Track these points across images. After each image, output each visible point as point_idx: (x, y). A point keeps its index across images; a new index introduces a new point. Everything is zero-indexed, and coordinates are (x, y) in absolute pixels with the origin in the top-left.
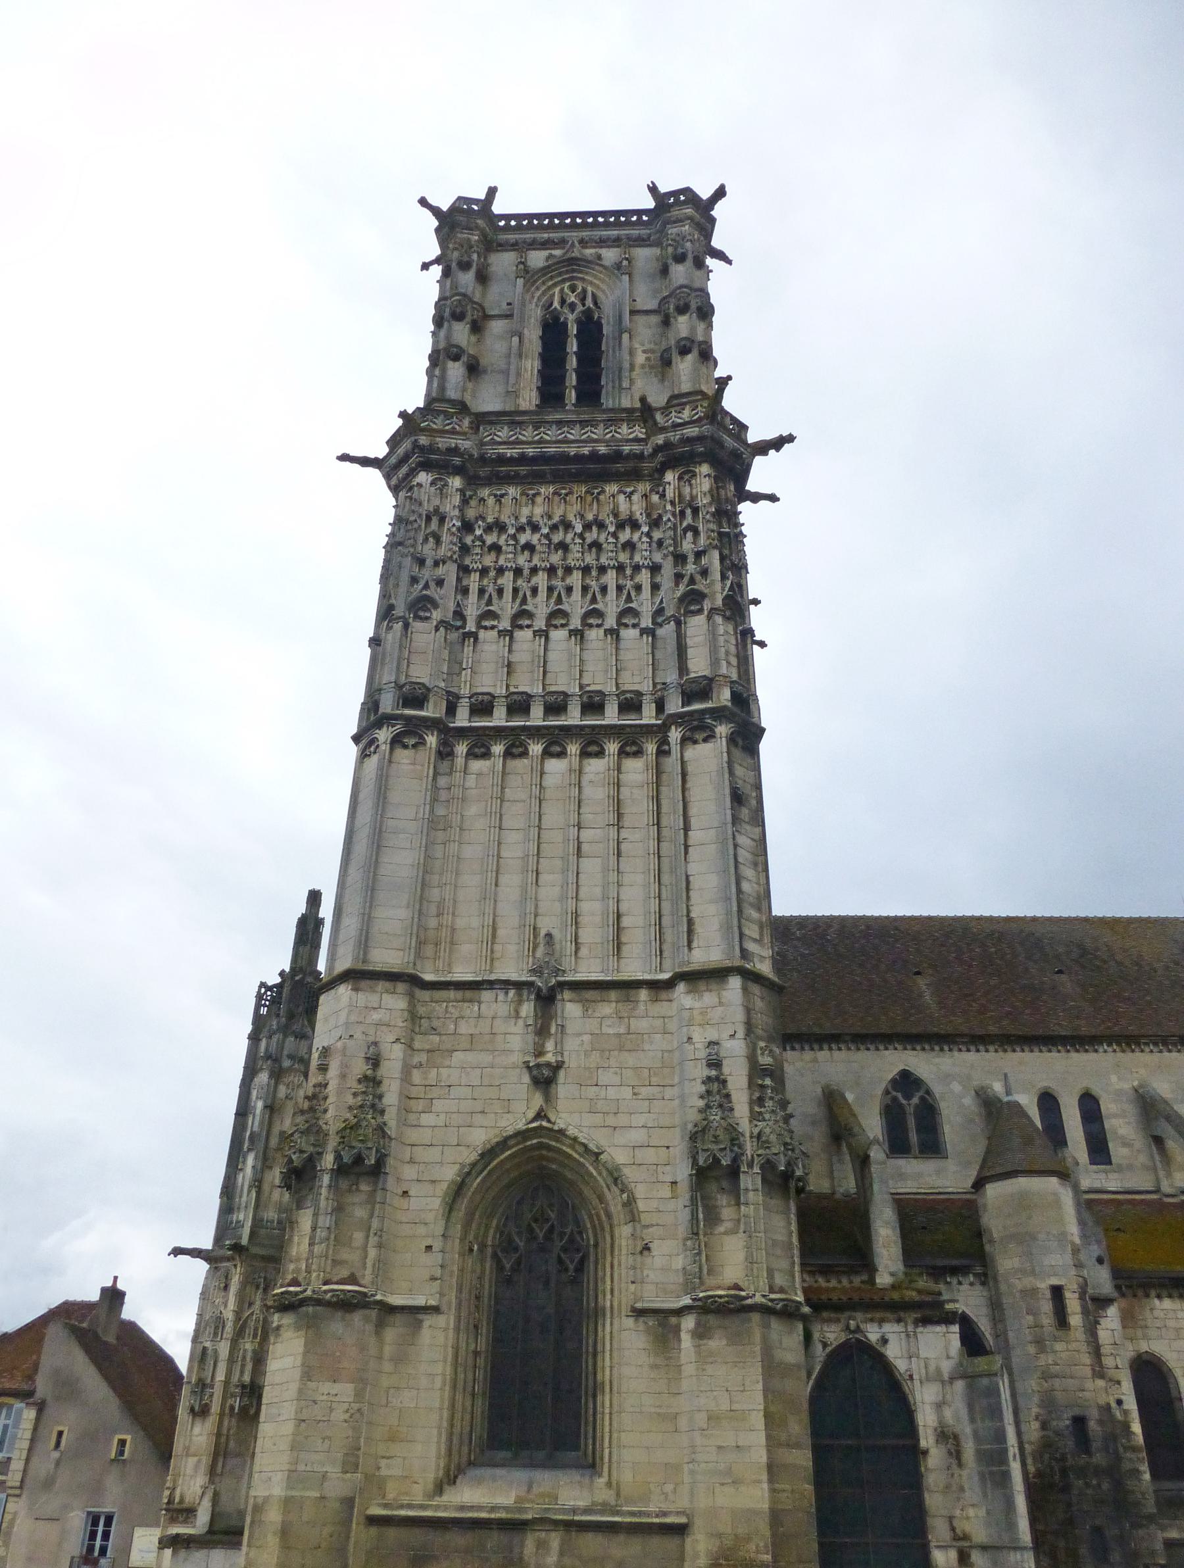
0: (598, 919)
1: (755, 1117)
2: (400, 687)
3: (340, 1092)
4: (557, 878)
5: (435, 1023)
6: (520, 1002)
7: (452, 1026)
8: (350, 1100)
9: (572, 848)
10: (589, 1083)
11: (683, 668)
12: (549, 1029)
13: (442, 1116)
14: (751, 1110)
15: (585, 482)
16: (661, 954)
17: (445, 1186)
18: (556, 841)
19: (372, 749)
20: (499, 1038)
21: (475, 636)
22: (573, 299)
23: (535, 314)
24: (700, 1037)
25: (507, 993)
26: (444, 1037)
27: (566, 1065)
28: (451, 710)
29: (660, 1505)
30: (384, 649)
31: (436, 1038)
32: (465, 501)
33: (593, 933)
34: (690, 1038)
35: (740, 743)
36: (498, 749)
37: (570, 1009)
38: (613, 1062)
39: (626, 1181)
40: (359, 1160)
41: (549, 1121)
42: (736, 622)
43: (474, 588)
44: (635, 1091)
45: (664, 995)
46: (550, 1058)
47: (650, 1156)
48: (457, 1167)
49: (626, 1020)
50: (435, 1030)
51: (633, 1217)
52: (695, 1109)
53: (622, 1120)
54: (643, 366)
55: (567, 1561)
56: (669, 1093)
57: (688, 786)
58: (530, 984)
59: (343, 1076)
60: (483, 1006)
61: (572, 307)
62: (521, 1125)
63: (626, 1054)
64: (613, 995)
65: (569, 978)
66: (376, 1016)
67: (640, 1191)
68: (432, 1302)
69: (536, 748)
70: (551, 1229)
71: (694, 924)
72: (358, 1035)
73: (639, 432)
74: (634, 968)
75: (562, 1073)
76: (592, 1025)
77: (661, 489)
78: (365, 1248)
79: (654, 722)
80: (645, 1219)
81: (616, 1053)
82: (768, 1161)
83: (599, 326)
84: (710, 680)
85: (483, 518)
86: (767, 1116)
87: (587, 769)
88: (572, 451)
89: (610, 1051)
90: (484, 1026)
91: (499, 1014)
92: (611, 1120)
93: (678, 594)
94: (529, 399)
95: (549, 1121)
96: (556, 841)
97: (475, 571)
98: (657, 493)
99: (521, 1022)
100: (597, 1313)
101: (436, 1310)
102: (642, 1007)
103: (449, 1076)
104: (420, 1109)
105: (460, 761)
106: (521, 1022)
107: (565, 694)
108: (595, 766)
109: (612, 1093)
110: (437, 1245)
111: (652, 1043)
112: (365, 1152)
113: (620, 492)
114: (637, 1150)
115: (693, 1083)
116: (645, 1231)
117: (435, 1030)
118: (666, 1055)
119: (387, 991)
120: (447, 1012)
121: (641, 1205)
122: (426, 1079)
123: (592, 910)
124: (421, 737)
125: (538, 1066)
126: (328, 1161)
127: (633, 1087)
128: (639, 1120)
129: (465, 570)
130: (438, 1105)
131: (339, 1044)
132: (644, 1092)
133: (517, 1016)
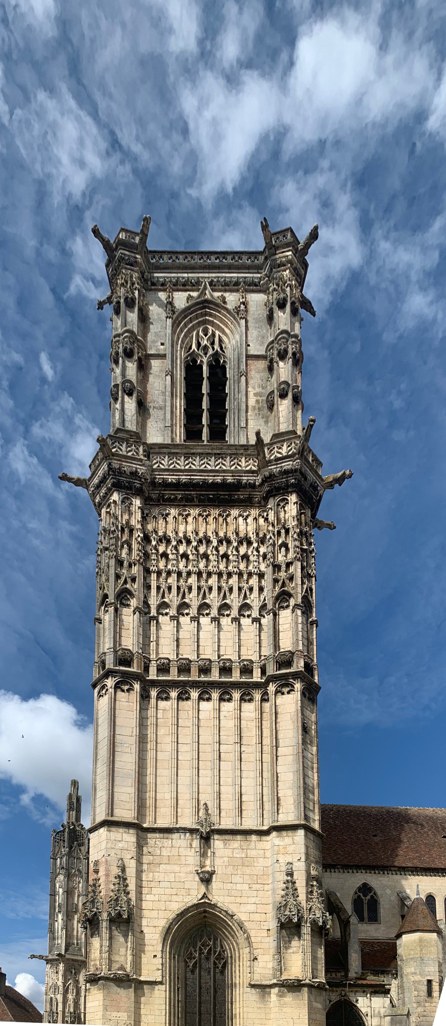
0: (230, 796)
1: (308, 900)
2: (115, 652)
3: (107, 882)
4: (209, 773)
6: (192, 840)
7: (159, 852)
8: (112, 887)
9: (216, 756)
10: (228, 881)
11: (276, 646)
12: (207, 853)
13: (157, 896)
14: (307, 897)
15: (218, 506)
16: (263, 816)
17: (161, 928)
18: (208, 753)
19: (104, 692)
20: (183, 858)
21: (156, 618)
22: (205, 342)
23: (181, 355)
24: (283, 860)
25: (185, 835)
26: (155, 857)
27: (216, 873)
28: (147, 669)
30: (104, 626)
31: (151, 857)
32: (144, 518)
33: (228, 804)
34: (277, 861)
35: (307, 695)
36: (174, 694)
37: (217, 843)
38: (239, 872)
39: (246, 929)
40: (119, 915)
41: (209, 899)
42: (307, 615)
43: (154, 584)
45: (264, 838)
46: (208, 869)
47: (257, 917)
51: (250, 944)
52: (280, 896)
53: (244, 900)
54: (254, 408)
56: (267, 888)
57: (278, 720)
58: (198, 830)
59: (107, 875)
60: (173, 841)
61: (205, 348)
62: (195, 902)
63: (246, 867)
64: (239, 837)
65: (216, 827)
66: (120, 845)
67: (252, 933)
68: (159, 979)
69: (195, 694)
70: (210, 949)
71: (280, 800)
72: (112, 855)
73: (252, 465)
74: (249, 823)
75: (214, 876)
76: (228, 852)
77: (265, 514)
78: (126, 955)
79: (259, 680)
80: (255, 946)
82: (314, 921)
83: (224, 368)
84: (292, 653)
85: (156, 533)
86: (314, 900)
87: (222, 709)
88: (210, 480)
90: (175, 852)
91: (182, 846)
92: (238, 900)
93: (276, 594)
94: (180, 436)
95: (209, 899)
96: (208, 753)
97: (154, 572)
98: (263, 517)
99: (193, 850)
100: (232, 986)
101: (161, 983)
102: (253, 843)
103: (159, 877)
105: (153, 701)
106: (193, 850)
107: (210, 660)
108: (227, 707)
109: (239, 887)
110: (159, 955)
112: (122, 913)
113: (240, 515)
114: (251, 914)
115: (279, 883)
116: (255, 951)
118: (265, 869)
119: (125, 832)
121: (253, 939)
123: (228, 792)
124: (131, 685)
125: (202, 872)
126: (105, 916)
127: (249, 884)
128: (253, 900)
129: (147, 572)
130: (154, 891)
131: (103, 859)
132: (255, 887)
133: (191, 847)
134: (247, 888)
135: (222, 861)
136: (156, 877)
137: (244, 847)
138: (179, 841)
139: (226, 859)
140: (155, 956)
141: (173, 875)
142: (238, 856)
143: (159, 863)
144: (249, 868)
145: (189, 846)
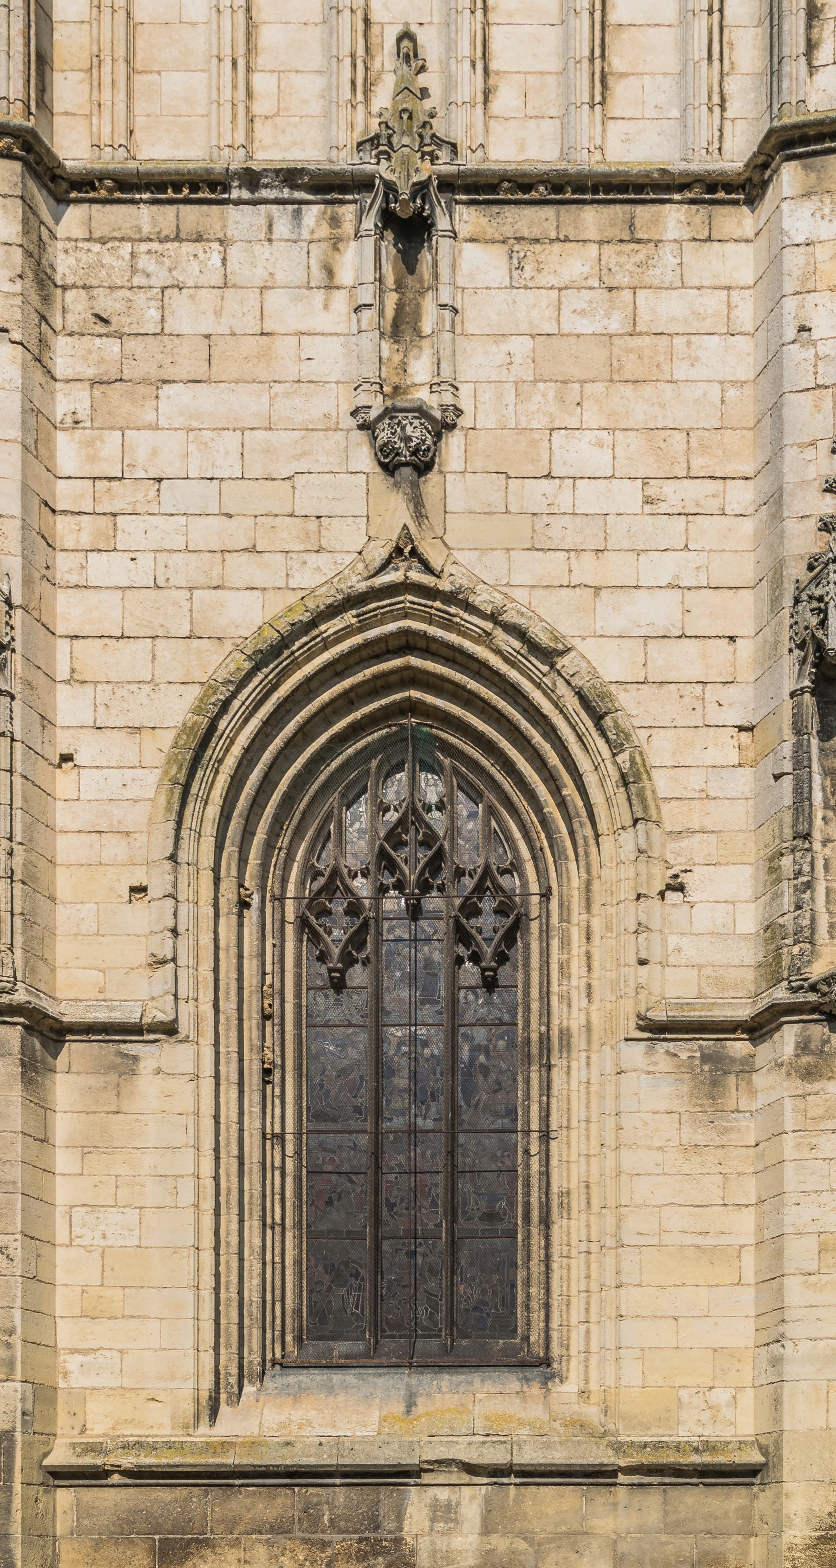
5: (106, 304)
6: (336, 243)
7: (154, 314)
10: (528, 469)
12: (417, 316)
13: (146, 561)
16: (722, 107)
17: (166, 739)
20: (285, 346)
26: (132, 344)
27: (465, 422)
29: (700, 1431)
31: (112, 347)
38: (592, 416)
39: (624, 723)
41: (428, 568)
44: (651, 491)
48: (196, 691)
49: (627, 295)
50: (106, 321)
55: (500, 1543)
60: (234, 252)
63: (627, 390)
75: (453, 444)
81: (600, 387)
89: (583, 382)
91: (281, 277)
95: (428, 568)
99: (340, 300)
102: (668, 256)
103: (154, 452)
104: (85, 540)
106: (340, 300)
111: (694, 361)
114: (652, 645)
116: (673, 846)
117: (106, 321)
118: (731, 393)
120: (134, 270)
122: (92, 459)
127: (646, 480)
133: (330, 284)
134: (635, 503)
135: (501, 358)
136: (141, 455)
137: (621, 279)
138: (263, 251)
139: (521, 346)
140: (139, 890)
141: (232, 440)
142: (585, 326)
143: (155, 374)
144: (647, 390)
145: (318, 276)
